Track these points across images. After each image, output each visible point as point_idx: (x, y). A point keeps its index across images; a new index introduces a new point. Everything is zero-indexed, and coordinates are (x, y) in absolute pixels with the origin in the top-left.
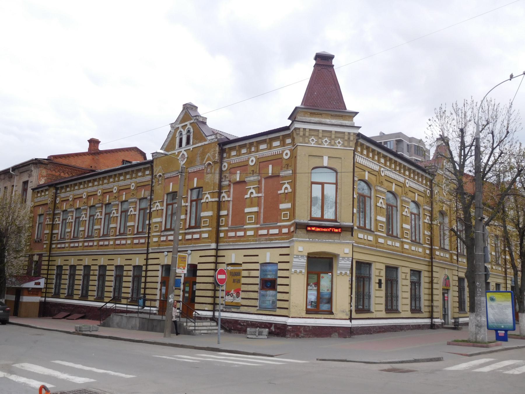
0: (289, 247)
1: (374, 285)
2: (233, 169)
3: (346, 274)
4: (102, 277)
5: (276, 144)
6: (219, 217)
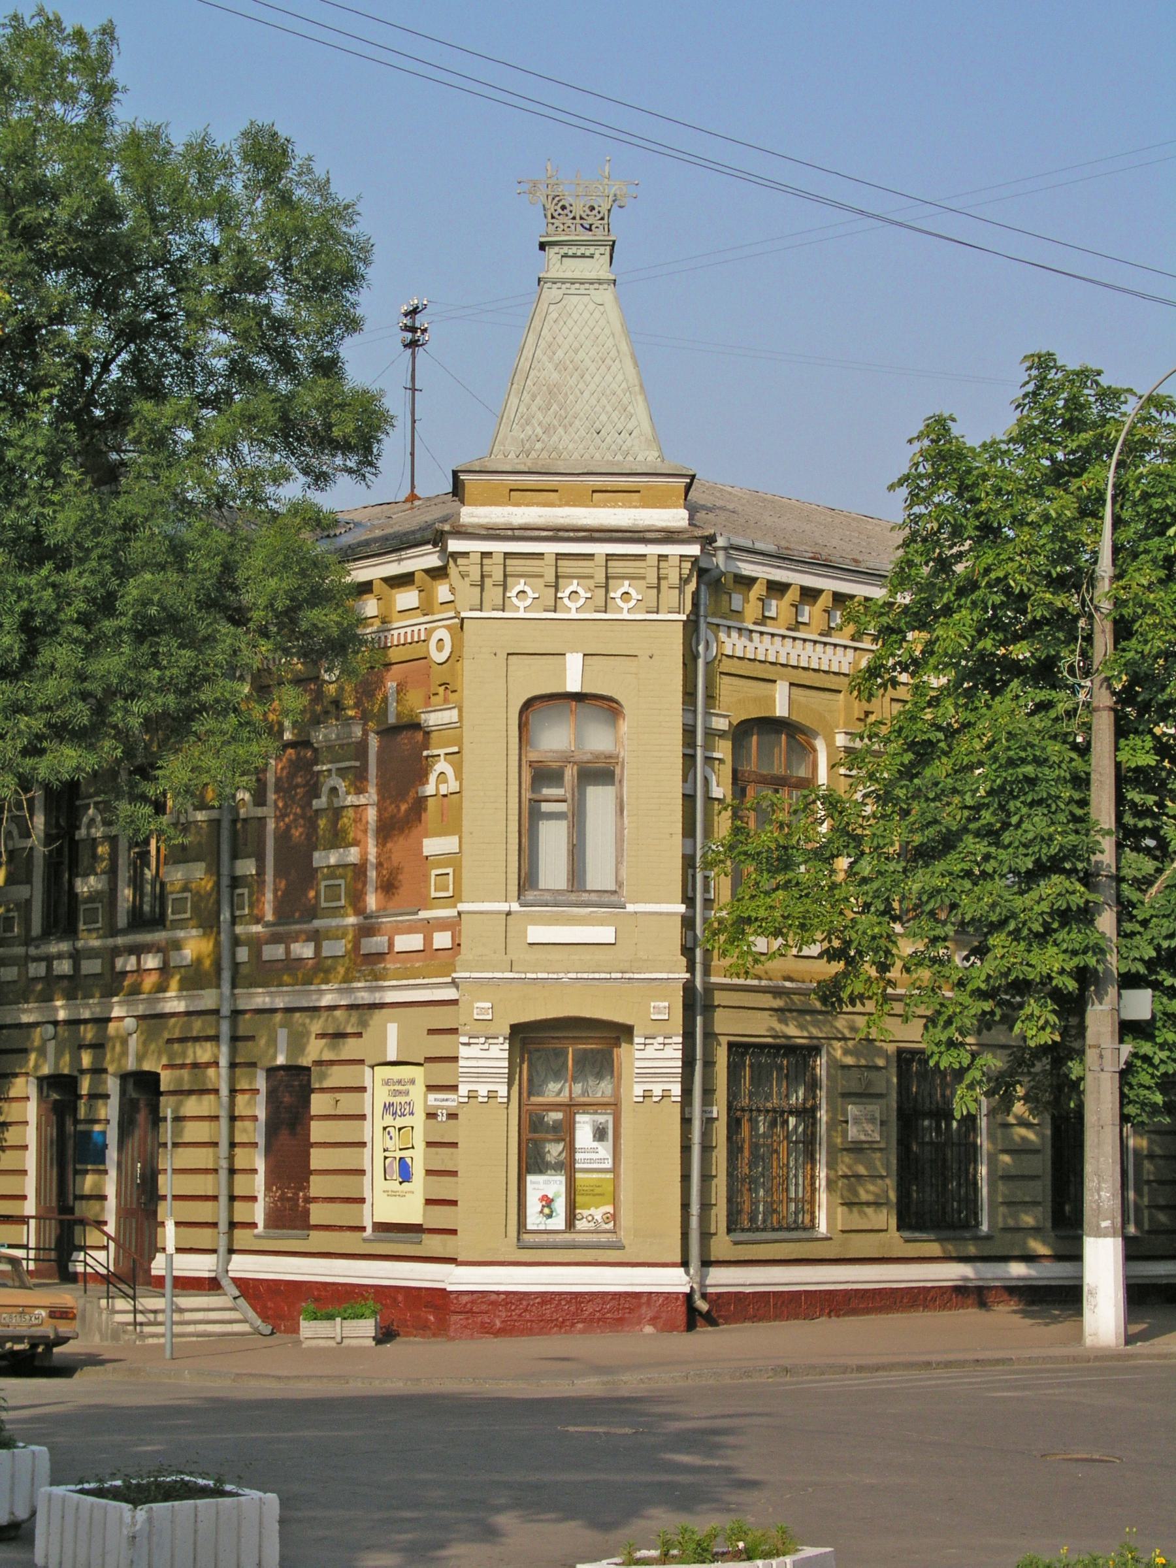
0: (454, 1002)
3: (666, 1095)
5: (407, 598)
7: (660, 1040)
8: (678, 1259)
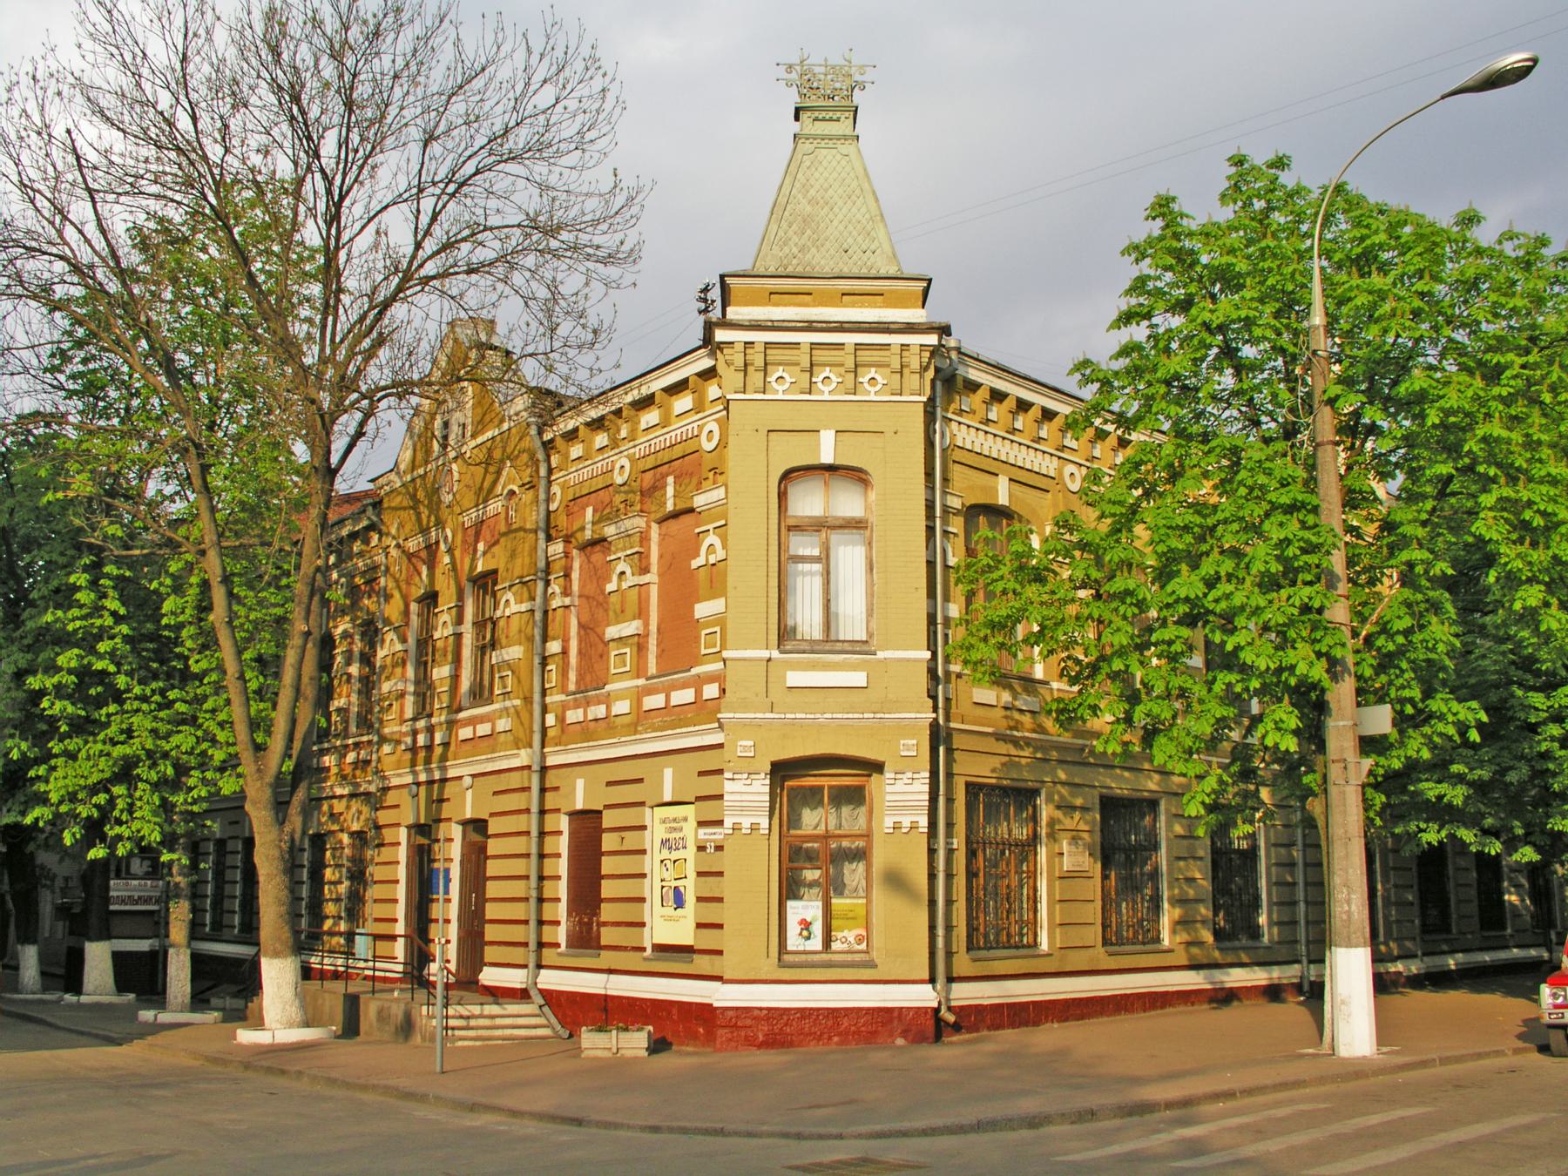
0: (721, 746)
3: (914, 826)
5: (683, 402)
7: (909, 775)
8: (926, 976)
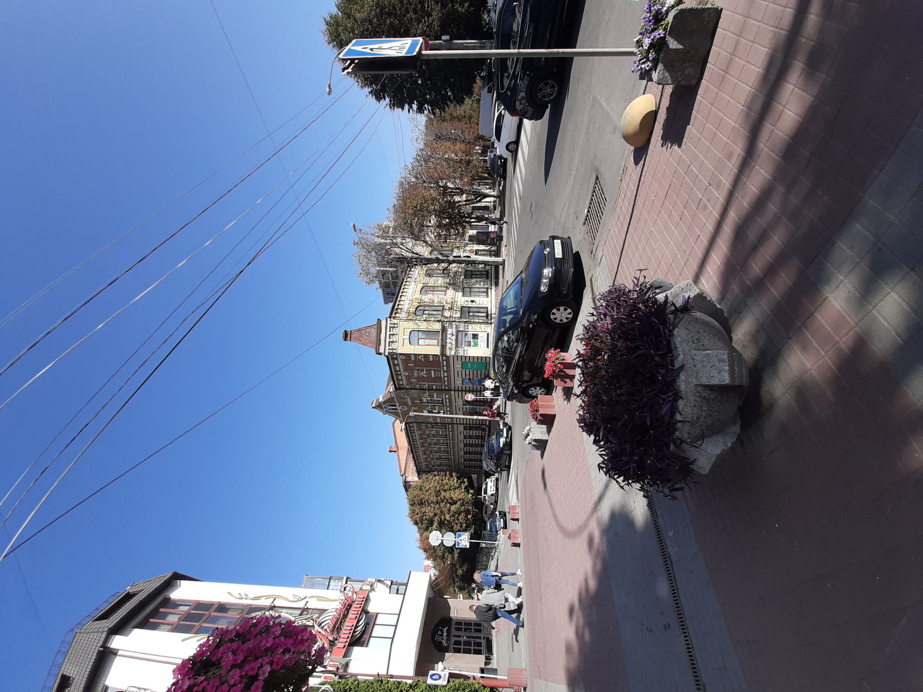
1: (474, 305)
2: (409, 382)
4: (470, 445)
6: (436, 390)
